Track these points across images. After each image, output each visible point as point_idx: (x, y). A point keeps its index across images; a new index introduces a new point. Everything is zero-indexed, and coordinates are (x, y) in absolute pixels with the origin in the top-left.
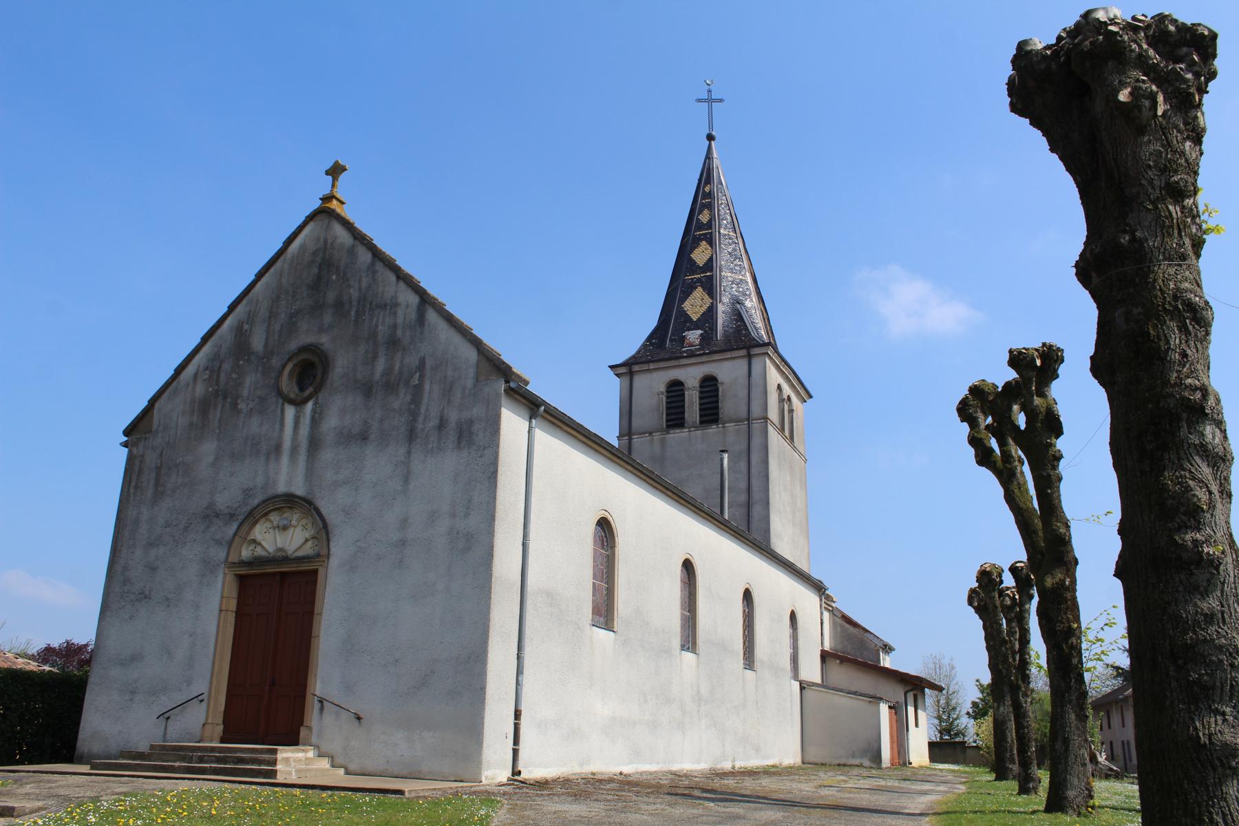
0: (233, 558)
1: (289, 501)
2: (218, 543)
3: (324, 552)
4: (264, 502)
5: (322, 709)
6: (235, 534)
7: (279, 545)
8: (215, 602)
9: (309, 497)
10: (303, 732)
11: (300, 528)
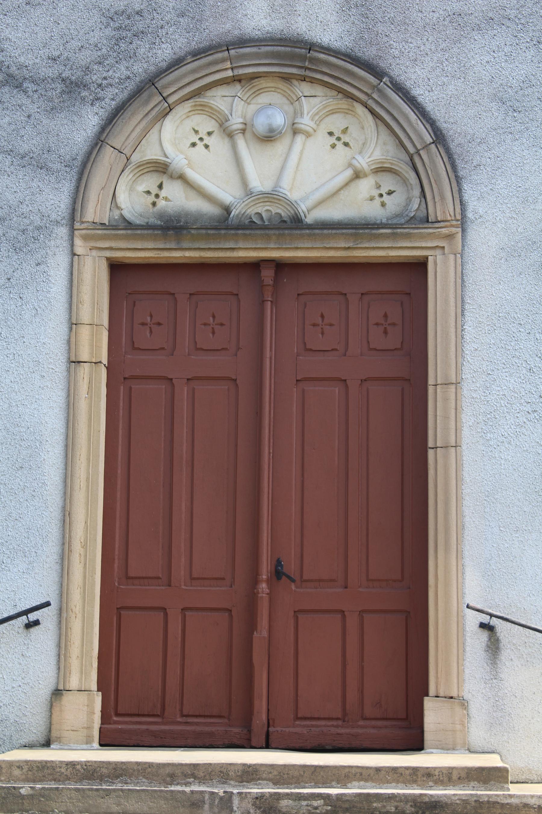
0: (95, 211)
1: (296, 60)
2: (36, 163)
4: (197, 54)
5: (494, 646)
6: (99, 141)
7: (258, 182)
9: (368, 53)
10: (434, 715)
11: (321, 140)
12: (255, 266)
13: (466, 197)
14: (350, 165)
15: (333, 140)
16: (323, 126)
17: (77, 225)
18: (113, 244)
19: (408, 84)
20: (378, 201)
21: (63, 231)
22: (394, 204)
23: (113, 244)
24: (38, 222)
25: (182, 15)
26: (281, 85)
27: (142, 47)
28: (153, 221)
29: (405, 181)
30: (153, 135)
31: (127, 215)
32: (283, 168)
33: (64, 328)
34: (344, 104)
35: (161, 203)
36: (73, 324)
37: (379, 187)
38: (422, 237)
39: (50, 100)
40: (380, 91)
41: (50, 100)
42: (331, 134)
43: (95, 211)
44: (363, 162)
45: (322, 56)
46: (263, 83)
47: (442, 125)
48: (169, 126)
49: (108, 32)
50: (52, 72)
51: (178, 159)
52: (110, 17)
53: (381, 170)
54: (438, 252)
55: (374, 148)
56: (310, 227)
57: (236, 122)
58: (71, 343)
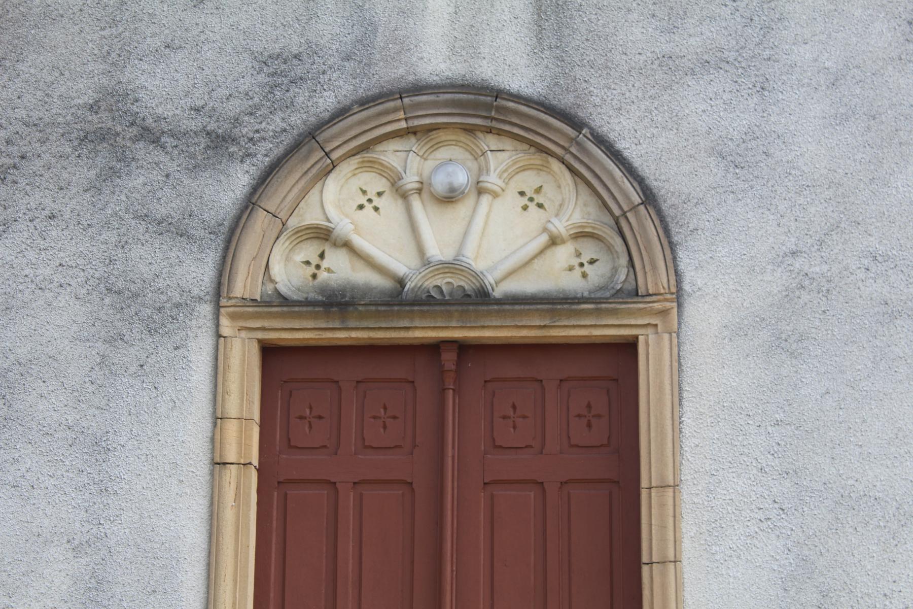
0: (245, 284)
1: (479, 109)
2: (177, 230)
3: (661, 280)
4: (365, 102)
6: (250, 203)
7: (437, 250)
8: (186, 431)
9: (565, 101)
11: (510, 202)
12: (434, 348)
13: (682, 266)
14: (545, 230)
15: (524, 201)
16: (512, 183)
17: (223, 302)
18: (266, 324)
19: (612, 136)
20: (578, 271)
21: (206, 309)
22: (597, 274)
23: (266, 324)
24: (177, 298)
25: (348, 58)
26: (463, 137)
27: (301, 96)
28: (312, 296)
29: (609, 248)
30: (313, 196)
31: (283, 289)
32: (466, 234)
33: (207, 424)
34: (537, 159)
35: (323, 276)
36: (218, 419)
37: (579, 255)
38: (631, 313)
39: (193, 156)
40: (579, 144)
41: (193, 156)
42: (522, 194)
43: (245, 284)
44: (561, 226)
45: (511, 105)
46: (442, 136)
47: (653, 183)
48: (332, 186)
49: (261, 78)
50: (194, 124)
51: (343, 225)
52: (264, 61)
53: (581, 235)
54: (650, 331)
55: (572, 210)
56: (499, 302)
57: (410, 181)
58: (215, 441)
